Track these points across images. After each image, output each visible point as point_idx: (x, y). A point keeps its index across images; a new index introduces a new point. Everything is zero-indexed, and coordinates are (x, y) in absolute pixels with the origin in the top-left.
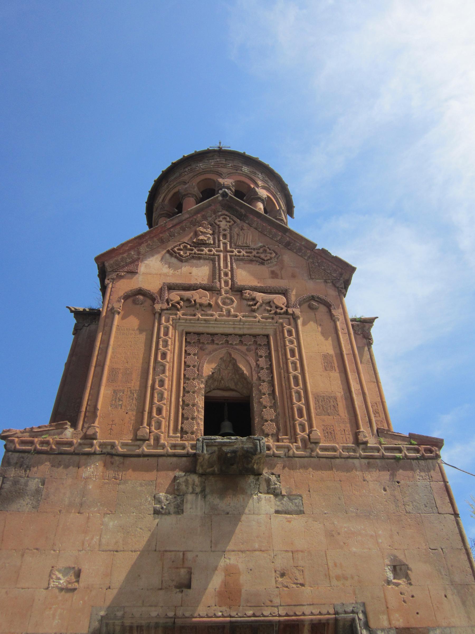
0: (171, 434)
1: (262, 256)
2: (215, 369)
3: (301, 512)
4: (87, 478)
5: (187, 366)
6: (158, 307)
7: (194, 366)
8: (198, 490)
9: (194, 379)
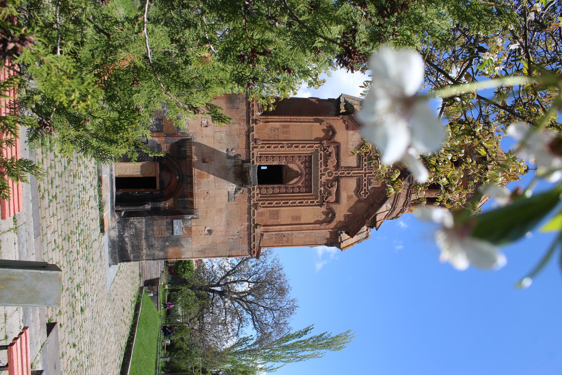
3: (229, 201)
5: (293, 157)
6: (325, 142)
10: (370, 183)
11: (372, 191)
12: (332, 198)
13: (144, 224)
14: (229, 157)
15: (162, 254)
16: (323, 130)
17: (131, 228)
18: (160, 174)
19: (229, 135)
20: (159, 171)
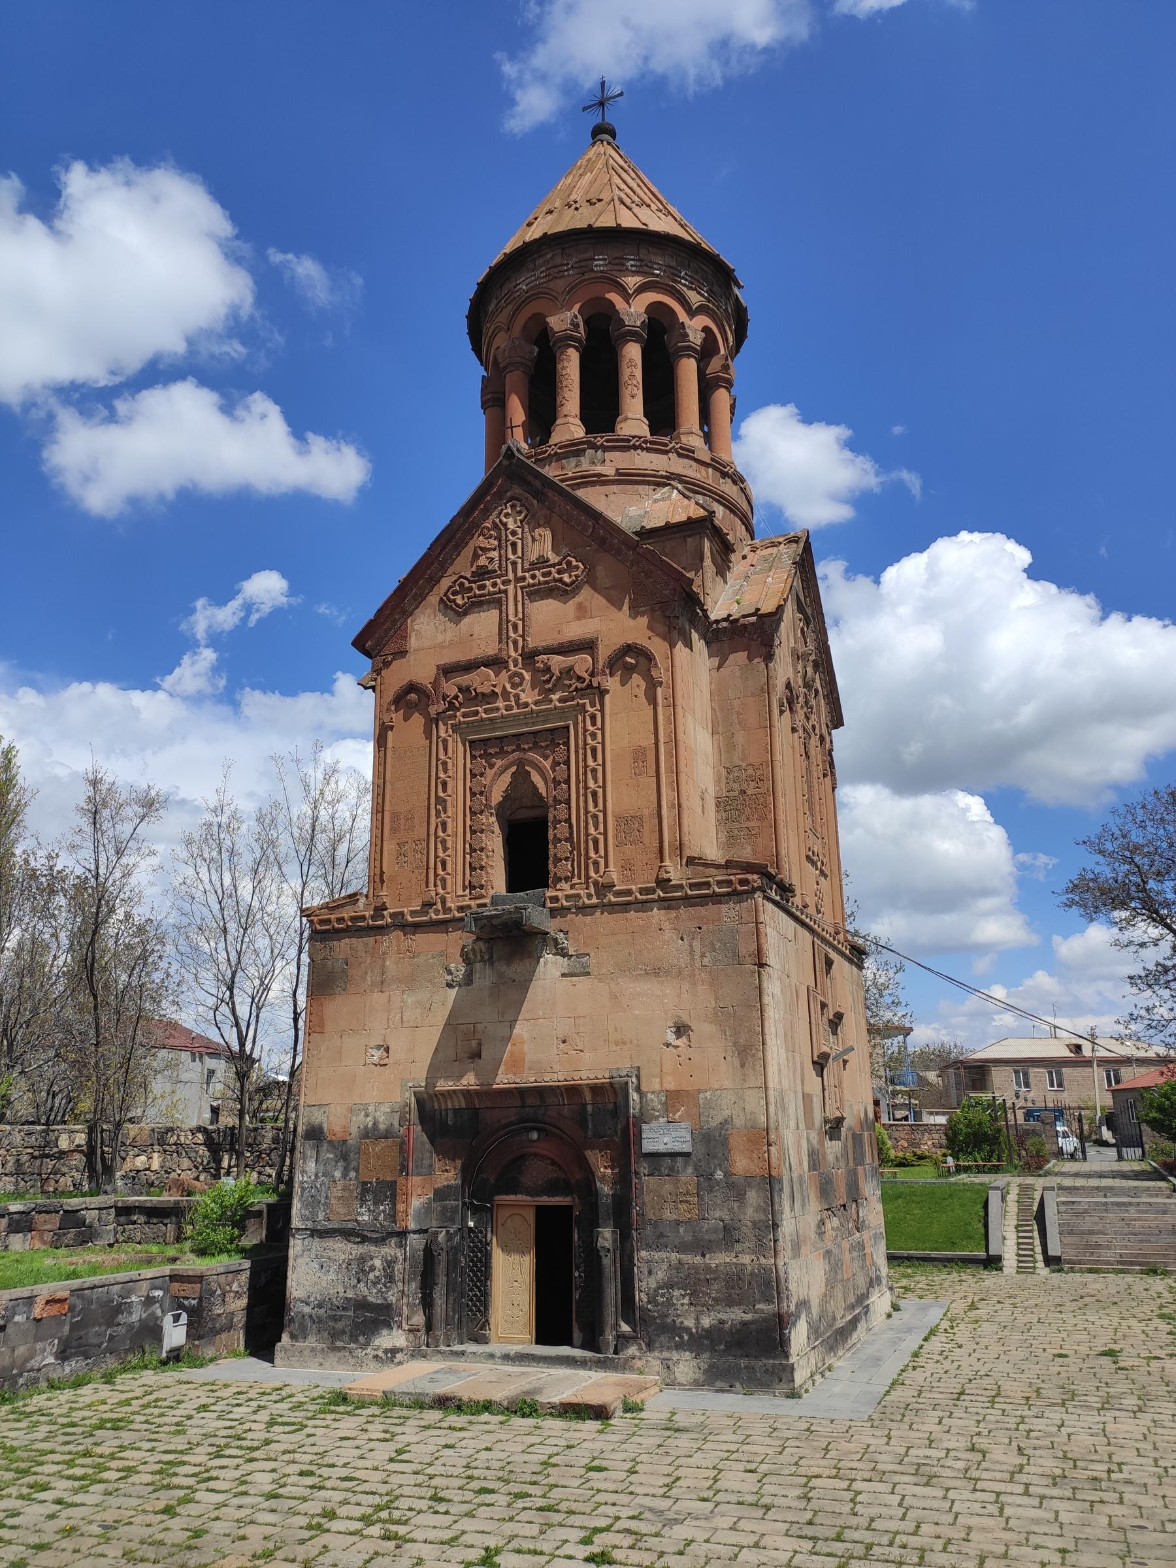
0: (460, 893)
1: (566, 578)
2: (507, 790)
3: (588, 974)
4: (384, 953)
5: (473, 794)
6: (433, 710)
7: (481, 793)
8: (486, 957)
9: (481, 813)
10: (542, 562)
11: (565, 550)
12: (582, 663)
13: (657, 1255)
14: (468, 980)
15: (753, 1197)
16: (406, 719)
17: (669, 1303)
18: (528, 1194)
19: (410, 982)
20: (519, 1197)
